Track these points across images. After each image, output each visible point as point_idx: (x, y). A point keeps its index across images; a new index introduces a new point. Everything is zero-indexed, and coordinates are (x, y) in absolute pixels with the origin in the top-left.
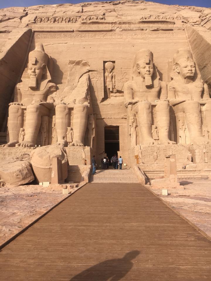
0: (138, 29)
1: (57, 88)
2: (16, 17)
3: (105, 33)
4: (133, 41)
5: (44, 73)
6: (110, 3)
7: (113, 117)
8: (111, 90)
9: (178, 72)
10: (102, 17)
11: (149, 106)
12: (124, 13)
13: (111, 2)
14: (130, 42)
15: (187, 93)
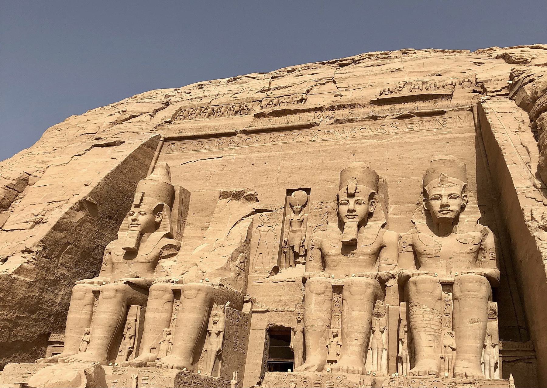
0: (367, 118)
1: (178, 249)
2: (145, 113)
3: (298, 132)
4: (353, 144)
5: (158, 220)
6: (334, 63)
7: (286, 309)
8: (296, 249)
9: (425, 210)
10: (300, 98)
11: (327, 287)
12: (351, 84)
13: (336, 61)
14: (348, 146)
15: (435, 257)
